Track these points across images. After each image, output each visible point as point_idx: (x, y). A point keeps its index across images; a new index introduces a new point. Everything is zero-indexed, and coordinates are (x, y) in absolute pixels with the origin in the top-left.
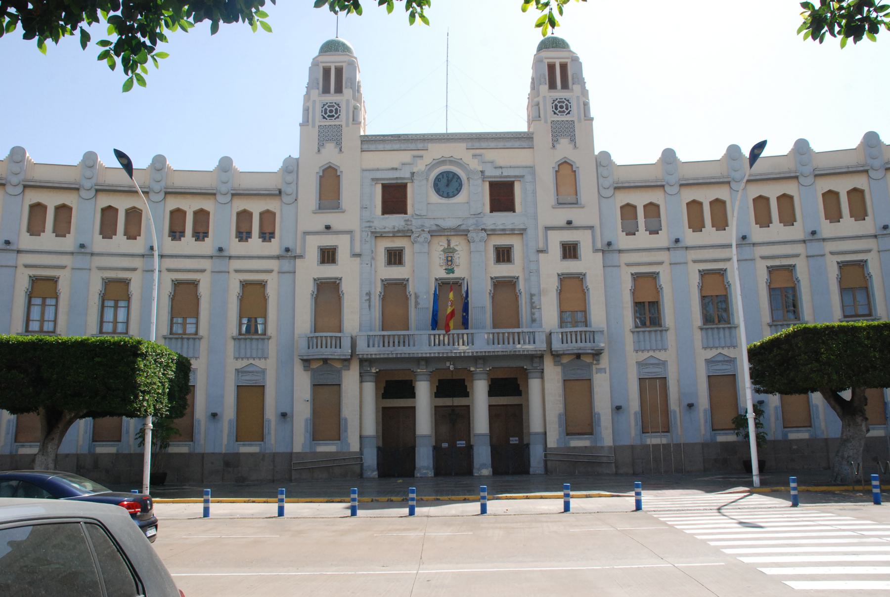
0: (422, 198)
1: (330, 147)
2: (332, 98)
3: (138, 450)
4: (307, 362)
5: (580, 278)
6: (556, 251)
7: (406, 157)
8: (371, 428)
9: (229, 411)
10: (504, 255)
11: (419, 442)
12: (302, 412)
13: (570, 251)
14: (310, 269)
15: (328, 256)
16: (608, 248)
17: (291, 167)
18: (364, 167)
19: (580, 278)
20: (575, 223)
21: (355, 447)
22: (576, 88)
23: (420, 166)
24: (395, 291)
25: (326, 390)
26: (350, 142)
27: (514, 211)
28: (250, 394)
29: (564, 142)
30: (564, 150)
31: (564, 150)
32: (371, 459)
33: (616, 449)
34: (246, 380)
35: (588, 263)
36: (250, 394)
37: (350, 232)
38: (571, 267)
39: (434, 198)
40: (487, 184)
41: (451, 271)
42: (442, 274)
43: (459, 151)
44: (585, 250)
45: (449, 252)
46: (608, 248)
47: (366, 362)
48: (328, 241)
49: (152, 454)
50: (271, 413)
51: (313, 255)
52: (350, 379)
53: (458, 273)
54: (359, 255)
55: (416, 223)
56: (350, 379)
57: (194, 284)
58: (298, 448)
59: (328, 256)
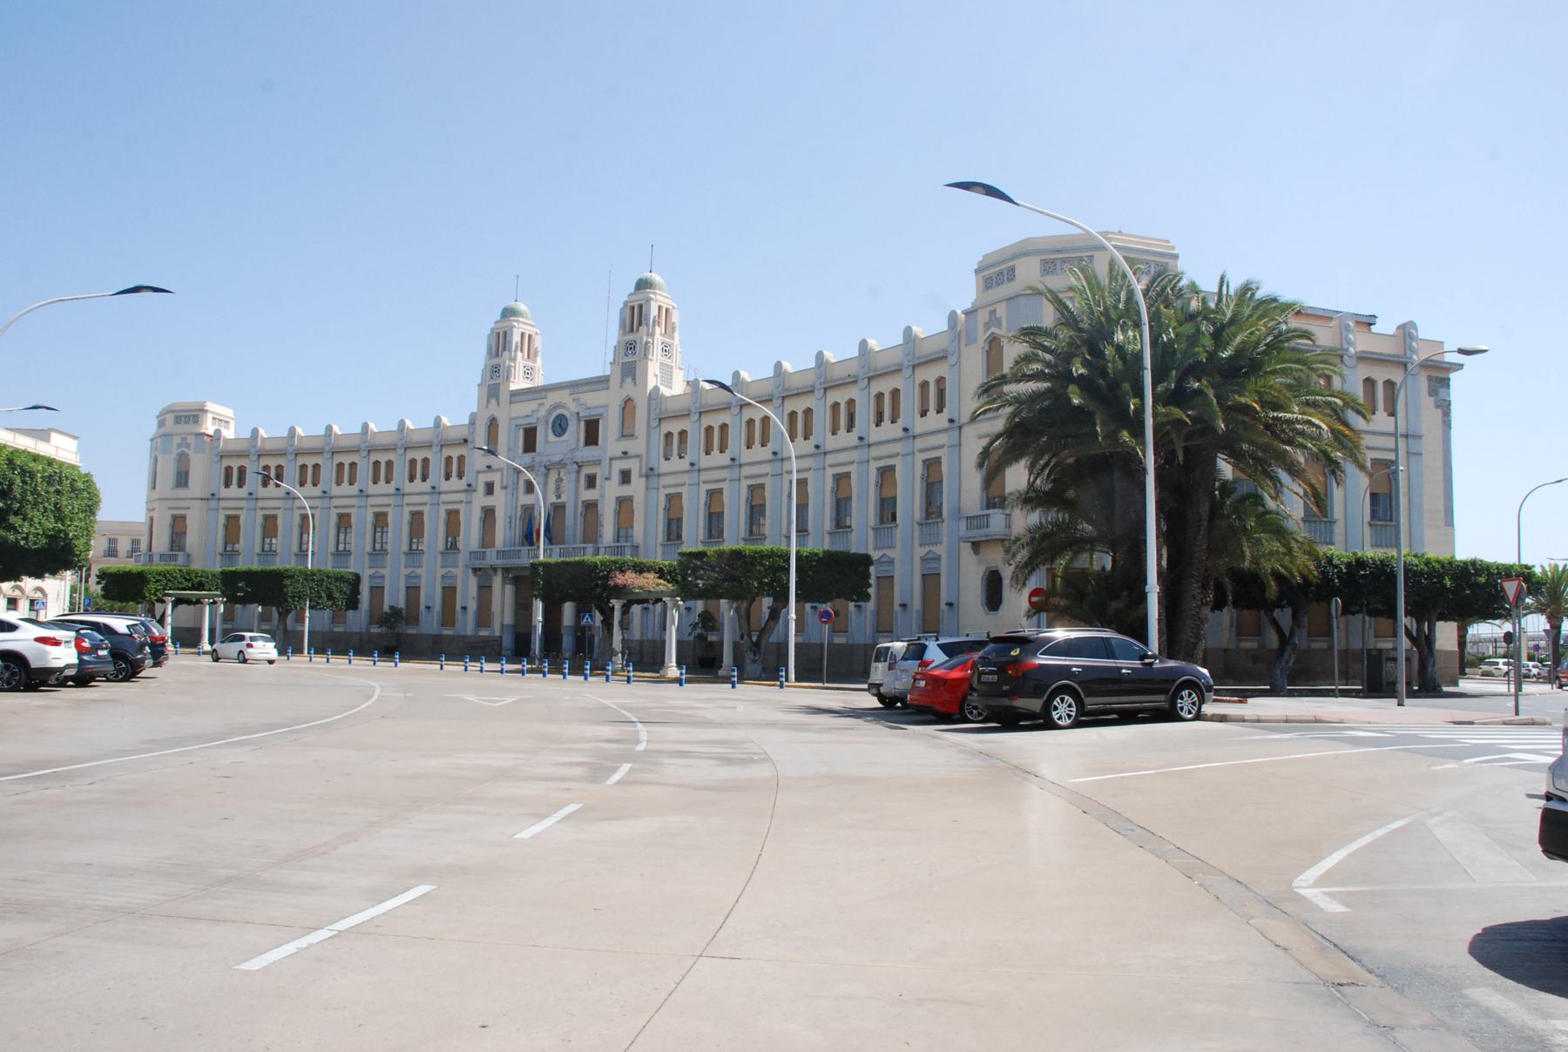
0: (544, 436)
1: (493, 401)
2: (496, 361)
3: (781, 639)
4: (475, 570)
5: (629, 499)
6: (616, 477)
7: (533, 405)
8: (508, 619)
9: (437, 606)
10: (591, 482)
11: (563, 631)
12: (472, 606)
13: (626, 477)
14: (480, 500)
15: (490, 489)
16: (650, 474)
17: (472, 422)
18: (514, 415)
19: (629, 499)
20: (631, 452)
21: (497, 633)
22: (643, 329)
23: (543, 412)
24: (529, 511)
25: (485, 589)
26: (504, 397)
27: (596, 443)
28: (449, 592)
29: (629, 380)
30: (629, 389)
31: (629, 389)
32: (508, 642)
33: (641, 642)
34: (448, 583)
35: (637, 488)
36: (449, 592)
37: (500, 470)
38: (626, 491)
39: (552, 437)
40: (582, 424)
41: (559, 497)
42: (553, 499)
43: (563, 397)
44: (634, 476)
45: (559, 480)
46: (650, 474)
47: (506, 570)
48: (489, 477)
49: (678, 642)
50: (458, 608)
51: (481, 489)
52: (497, 581)
53: (563, 499)
54: (505, 488)
55: (538, 459)
56: (497, 581)
57: (421, 513)
58: (470, 631)
59: (490, 489)
